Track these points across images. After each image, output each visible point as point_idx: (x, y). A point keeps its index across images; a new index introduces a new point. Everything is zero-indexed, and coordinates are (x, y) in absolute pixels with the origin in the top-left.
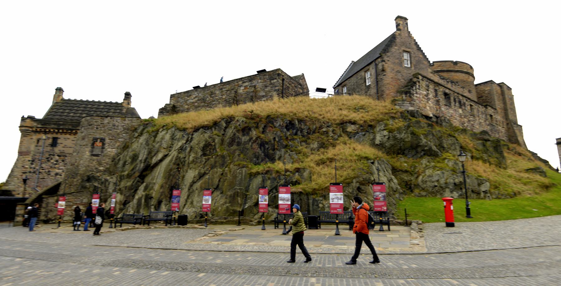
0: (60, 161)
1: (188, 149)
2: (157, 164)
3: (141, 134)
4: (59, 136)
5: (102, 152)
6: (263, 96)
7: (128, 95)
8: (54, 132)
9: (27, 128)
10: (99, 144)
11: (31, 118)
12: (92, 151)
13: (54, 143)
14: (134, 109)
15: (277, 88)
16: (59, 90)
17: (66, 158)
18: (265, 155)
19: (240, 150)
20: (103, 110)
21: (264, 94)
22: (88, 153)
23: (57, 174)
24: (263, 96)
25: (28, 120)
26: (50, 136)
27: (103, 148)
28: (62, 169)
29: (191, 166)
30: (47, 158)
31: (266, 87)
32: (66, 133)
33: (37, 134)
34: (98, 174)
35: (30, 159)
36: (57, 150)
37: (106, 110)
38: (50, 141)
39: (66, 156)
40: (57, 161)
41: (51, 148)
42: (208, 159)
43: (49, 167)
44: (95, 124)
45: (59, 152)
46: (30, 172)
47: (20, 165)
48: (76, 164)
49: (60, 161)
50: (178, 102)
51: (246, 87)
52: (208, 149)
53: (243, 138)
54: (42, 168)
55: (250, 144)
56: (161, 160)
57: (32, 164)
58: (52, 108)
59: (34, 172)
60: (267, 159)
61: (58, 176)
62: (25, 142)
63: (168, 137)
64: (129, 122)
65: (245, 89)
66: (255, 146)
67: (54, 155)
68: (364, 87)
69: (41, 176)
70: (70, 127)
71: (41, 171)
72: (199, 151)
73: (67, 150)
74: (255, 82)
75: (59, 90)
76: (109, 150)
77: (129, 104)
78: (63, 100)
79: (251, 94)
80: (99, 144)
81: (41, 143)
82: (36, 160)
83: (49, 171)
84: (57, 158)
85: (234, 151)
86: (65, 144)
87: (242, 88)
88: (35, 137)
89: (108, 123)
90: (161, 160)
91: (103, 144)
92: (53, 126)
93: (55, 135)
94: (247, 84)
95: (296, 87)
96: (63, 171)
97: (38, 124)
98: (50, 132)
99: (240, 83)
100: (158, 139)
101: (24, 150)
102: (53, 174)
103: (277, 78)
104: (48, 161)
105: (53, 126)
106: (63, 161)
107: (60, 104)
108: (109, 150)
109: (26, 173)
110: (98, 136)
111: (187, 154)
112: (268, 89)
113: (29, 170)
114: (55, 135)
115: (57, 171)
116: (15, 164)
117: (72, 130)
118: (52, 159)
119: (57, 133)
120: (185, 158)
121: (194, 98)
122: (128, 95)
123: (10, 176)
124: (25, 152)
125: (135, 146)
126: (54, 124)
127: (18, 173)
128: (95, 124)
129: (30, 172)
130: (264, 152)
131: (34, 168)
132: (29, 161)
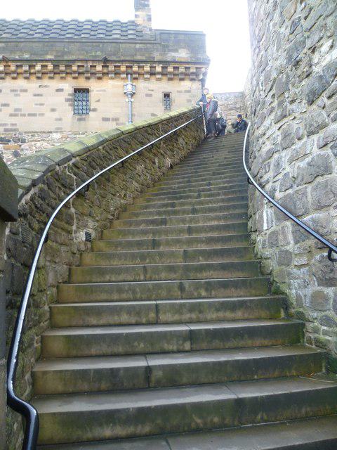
17: (24, 146)
32: (16, 75)
39: (24, 141)
70: (26, 56)
73: (23, 124)
86: (14, 105)
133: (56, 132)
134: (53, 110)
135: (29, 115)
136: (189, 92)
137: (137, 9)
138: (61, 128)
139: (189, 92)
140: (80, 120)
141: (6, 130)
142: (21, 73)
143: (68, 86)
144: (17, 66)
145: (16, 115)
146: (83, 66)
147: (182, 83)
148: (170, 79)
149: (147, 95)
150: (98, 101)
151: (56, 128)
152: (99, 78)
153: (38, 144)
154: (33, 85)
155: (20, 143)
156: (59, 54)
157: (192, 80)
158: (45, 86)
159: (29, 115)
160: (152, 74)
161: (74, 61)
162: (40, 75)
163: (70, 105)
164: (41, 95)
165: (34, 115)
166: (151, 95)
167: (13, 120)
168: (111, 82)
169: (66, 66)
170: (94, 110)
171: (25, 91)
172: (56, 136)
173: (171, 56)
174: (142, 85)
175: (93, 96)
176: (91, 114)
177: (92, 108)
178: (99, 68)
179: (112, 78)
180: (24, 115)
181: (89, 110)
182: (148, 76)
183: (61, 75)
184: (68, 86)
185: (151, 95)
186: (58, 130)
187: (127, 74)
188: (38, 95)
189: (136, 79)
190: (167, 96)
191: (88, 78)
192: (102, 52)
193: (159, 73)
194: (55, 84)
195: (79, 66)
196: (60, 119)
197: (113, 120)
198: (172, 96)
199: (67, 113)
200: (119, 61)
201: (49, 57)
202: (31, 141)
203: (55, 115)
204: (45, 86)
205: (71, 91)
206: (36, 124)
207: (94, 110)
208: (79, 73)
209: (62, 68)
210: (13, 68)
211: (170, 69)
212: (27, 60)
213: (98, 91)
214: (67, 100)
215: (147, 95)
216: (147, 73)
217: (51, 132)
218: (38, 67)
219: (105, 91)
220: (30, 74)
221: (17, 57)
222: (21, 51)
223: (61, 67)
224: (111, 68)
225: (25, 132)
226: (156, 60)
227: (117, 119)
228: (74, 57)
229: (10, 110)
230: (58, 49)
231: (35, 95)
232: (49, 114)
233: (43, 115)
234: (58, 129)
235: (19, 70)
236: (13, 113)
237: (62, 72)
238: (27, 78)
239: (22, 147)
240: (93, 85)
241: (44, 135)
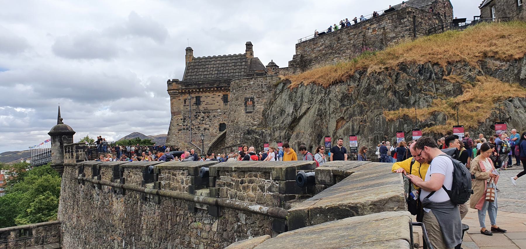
0: (206, 117)
1: (328, 101)
2: (301, 117)
3: (282, 91)
5: (254, 109)
6: (394, 38)
7: (249, 46)
8: (196, 91)
10: (250, 102)
11: (176, 81)
12: (246, 110)
13: (198, 102)
14: (257, 59)
15: (408, 27)
16: (189, 50)
17: (210, 114)
18: (400, 101)
19: (376, 99)
20: (231, 65)
21: (394, 35)
22: (243, 111)
23: (205, 129)
24: (394, 38)
25: (174, 83)
26: (193, 95)
27: (254, 106)
29: (332, 116)
30: (196, 116)
31: (396, 27)
32: (206, 92)
34: (255, 127)
36: (201, 108)
37: (233, 64)
38: (194, 100)
40: (203, 117)
42: (348, 109)
44: (244, 85)
46: (184, 129)
48: (236, 121)
49: (206, 117)
50: (305, 51)
51: (374, 30)
52: (346, 100)
53: (377, 87)
55: (385, 92)
56: (305, 113)
57: (184, 122)
58: (187, 69)
59: (187, 129)
60: (402, 105)
61: (206, 131)
62: (175, 103)
63: (307, 92)
64: (270, 80)
65: (373, 31)
66: (390, 94)
68: (515, 8)
69: (193, 132)
72: (338, 102)
73: (210, 107)
74: (383, 23)
75: (189, 50)
76: (258, 107)
77: (252, 54)
78: (194, 59)
79: (381, 37)
80: (250, 102)
81: (187, 103)
84: (203, 114)
85: (370, 100)
86: (206, 102)
87: (370, 31)
88: (182, 98)
89: (254, 84)
90: (305, 113)
91: (254, 103)
92: (194, 86)
93: (197, 95)
94: (375, 26)
95: (429, 19)
99: (368, 25)
100: (299, 94)
101: (176, 110)
102: (202, 129)
103: (407, 16)
104: (196, 118)
106: (208, 117)
107: (192, 64)
108: (258, 107)
109: (181, 130)
110: (248, 96)
111: (327, 105)
112: (399, 29)
114: (197, 95)
115: (205, 126)
117: (210, 88)
118: (199, 116)
119: (198, 92)
120: (325, 109)
121: (321, 46)
122: (249, 46)
125: (279, 101)
126: (195, 84)
127: (175, 130)
128: (244, 85)
129: (184, 129)
130: (399, 98)
137: (246, 51)
143: (221, 94)
154: (211, 95)
167: (206, 106)
172: (219, 110)
184: (221, 94)
186: (220, 109)
194: (218, 94)
201: (215, 86)
203: (218, 104)
206: (213, 107)
223: (219, 89)
229: (205, 103)
232: (216, 104)
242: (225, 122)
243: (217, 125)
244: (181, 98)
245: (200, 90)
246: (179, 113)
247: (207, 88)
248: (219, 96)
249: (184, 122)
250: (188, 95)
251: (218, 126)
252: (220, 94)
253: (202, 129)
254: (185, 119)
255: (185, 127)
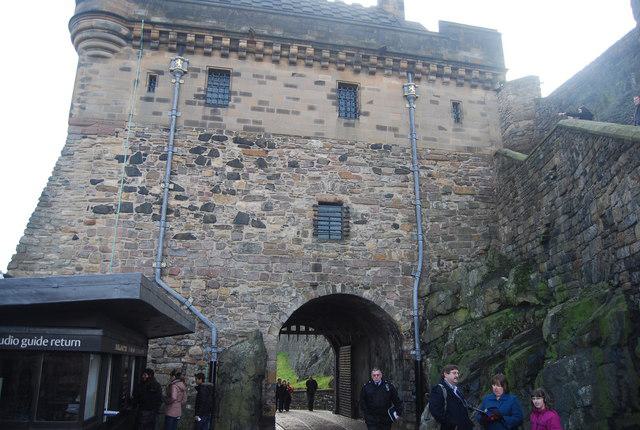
4: (232, 63)
9: (111, 23)
23: (241, 220)
26: (199, 61)
28: (263, 198)
33: (148, 53)
35: (125, 151)
36: (231, 119)
38: (202, 81)
39: (272, 146)
40: (236, 164)
41: (208, 111)
43: (207, 189)
45: (241, 127)
46: (127, 208)
47: (80, 175)
54: (179, 192)
57: (133, 172)
59: (145, 209)
61: (247, 229)
67: (221, 139)
70: (278, 33)
71: (174, 203)
73: (271, 124)
81: (161, 90)
82: (149, 159)
83: (207, 207)
84: (237, 150)
96: (267, 208)
97: (153, 12)
98: (199, 47)
101: (94, 110)
104: (201, 161)
105: (211, 23)
106: (261, 164)
109: (109, 210)
113: (120, 197)
114: (216, 61)
115: (242, 206)
116: (57, 169)
118: (214, 154)
123: (34, 225)
124: (102, 122)
127: (73, 208)
129: (127, 208)
131: (144, 191)
132: (120, 159)
133: (316, 138)
134: (311, 108)
135: (279, 111)
136: (483, 103)
138: (323, 134)
139: (483, 103)
140: (347, 125)
141: (246, 128)
142: (268, 54)
143: (331, 78)
144: (265, 44)
145: (260, 110)
146: (353, 55)
147: (474, 91)
148: (460, 85)
149: (432, 102)
150: (371, 102)
151: (317, 133)
152: (373, 73)
153: (293, 153)
154: (284, 72)
155: (266, 149)
156: (323, 36)
157: (487, 89)
158: (301, 75)
159: (279, 111)
160: (439, 75)
161: (342, 47)
162: (295, 59)
163: (333, 104)
164: (295, 87)
165: (287, 112)
166: (436, 103)
167: (257, 116)
168: (386, 80)
169: (331, 52)
170: (366, 114)
171: (273, 78)
172: (317, 143)
173: (462, 55)
174: (424, 86)
175: (364, 96)
176: (361, 117)
177: (363, 110)
178: (373, 60)
179: (388, 75)
180: (272, 111)
181: (356, 114)
182: (434, 78)
183: (323, 64)
184: (331, 78)
185: (436, 103)
187: (408, 72)
188: (291, 86)
189: (419, 79)
190: (456, 105)
191: (357, 72)
192: (377, 40)
193: (447, 76)
194: (314, 74)
195: (347, 54)
196: (321, 122)
197: (391, 129)
198: (464, 106)
199: (331, 115)
200: (399, 55)
202: (283, 148)
203: (314, 115)
204: (301, 75)
205: (335, 85)
207: (366, 114)
208: (347, 64)
209: (326, 54)
210: (260, 45)
211: (462, 72)
212: (279, 38)
213: (369, 89)
214: (330, 97)
215: (432, 102)
216: (433, 73)
217: (309, 138)
218: (294, 50)
219: (378, 90)
220: (281, 56)
221: (266, 32)
222: (271, 24)
224: (389, 62)
225: (274, 135)
226: (445, 58)
227: (395, 130)
228: (342, 42)
229: (253, 102)
230: (320, 28)
231: (287, 86)
232: (305, 113)
233: (297, 113)
234: (320, 134)
235: (267, 51)
236: (256, 105)
237: (325, 59)
238: (276, 62)
239: (270, 154)
240: (363, 80)
241: (301, 141)
242: (346, 199)
243: (304, 204)
244: (133, 63)
245: (234, 41)
246: (110, 127)
247: (270, 40)
248: (321, 83)
249: (133, 172)
250: (169, 56)
251: (310, 213)
252: (322, 76)
253: (224, 217)
254: (138, 159)
255: (134, 199)
